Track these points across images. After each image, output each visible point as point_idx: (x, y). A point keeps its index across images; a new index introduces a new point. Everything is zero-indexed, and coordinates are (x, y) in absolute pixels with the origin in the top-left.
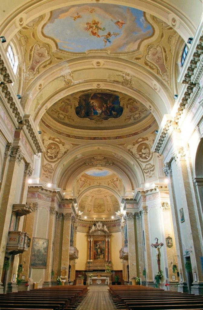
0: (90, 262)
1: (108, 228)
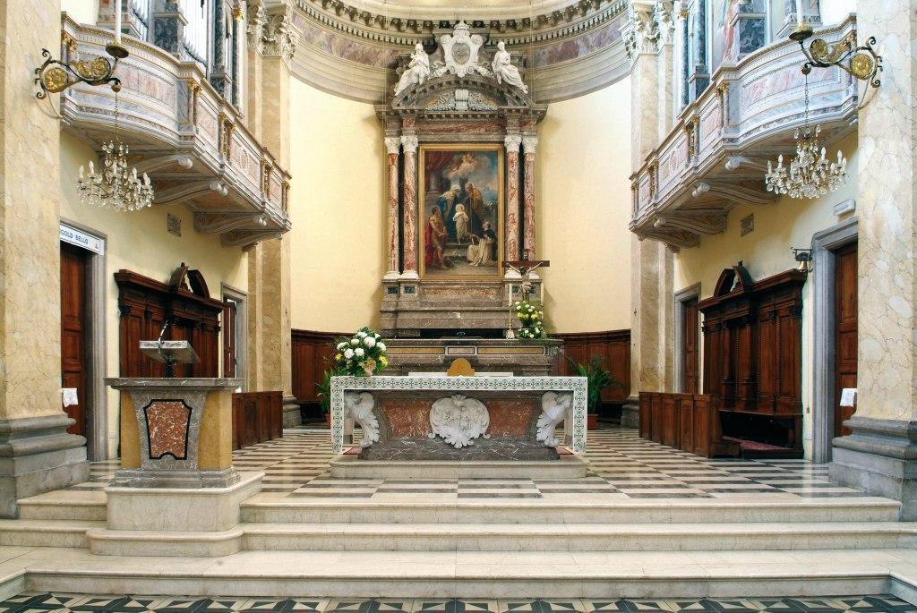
0: (399, 283)
1: (524, 64)
